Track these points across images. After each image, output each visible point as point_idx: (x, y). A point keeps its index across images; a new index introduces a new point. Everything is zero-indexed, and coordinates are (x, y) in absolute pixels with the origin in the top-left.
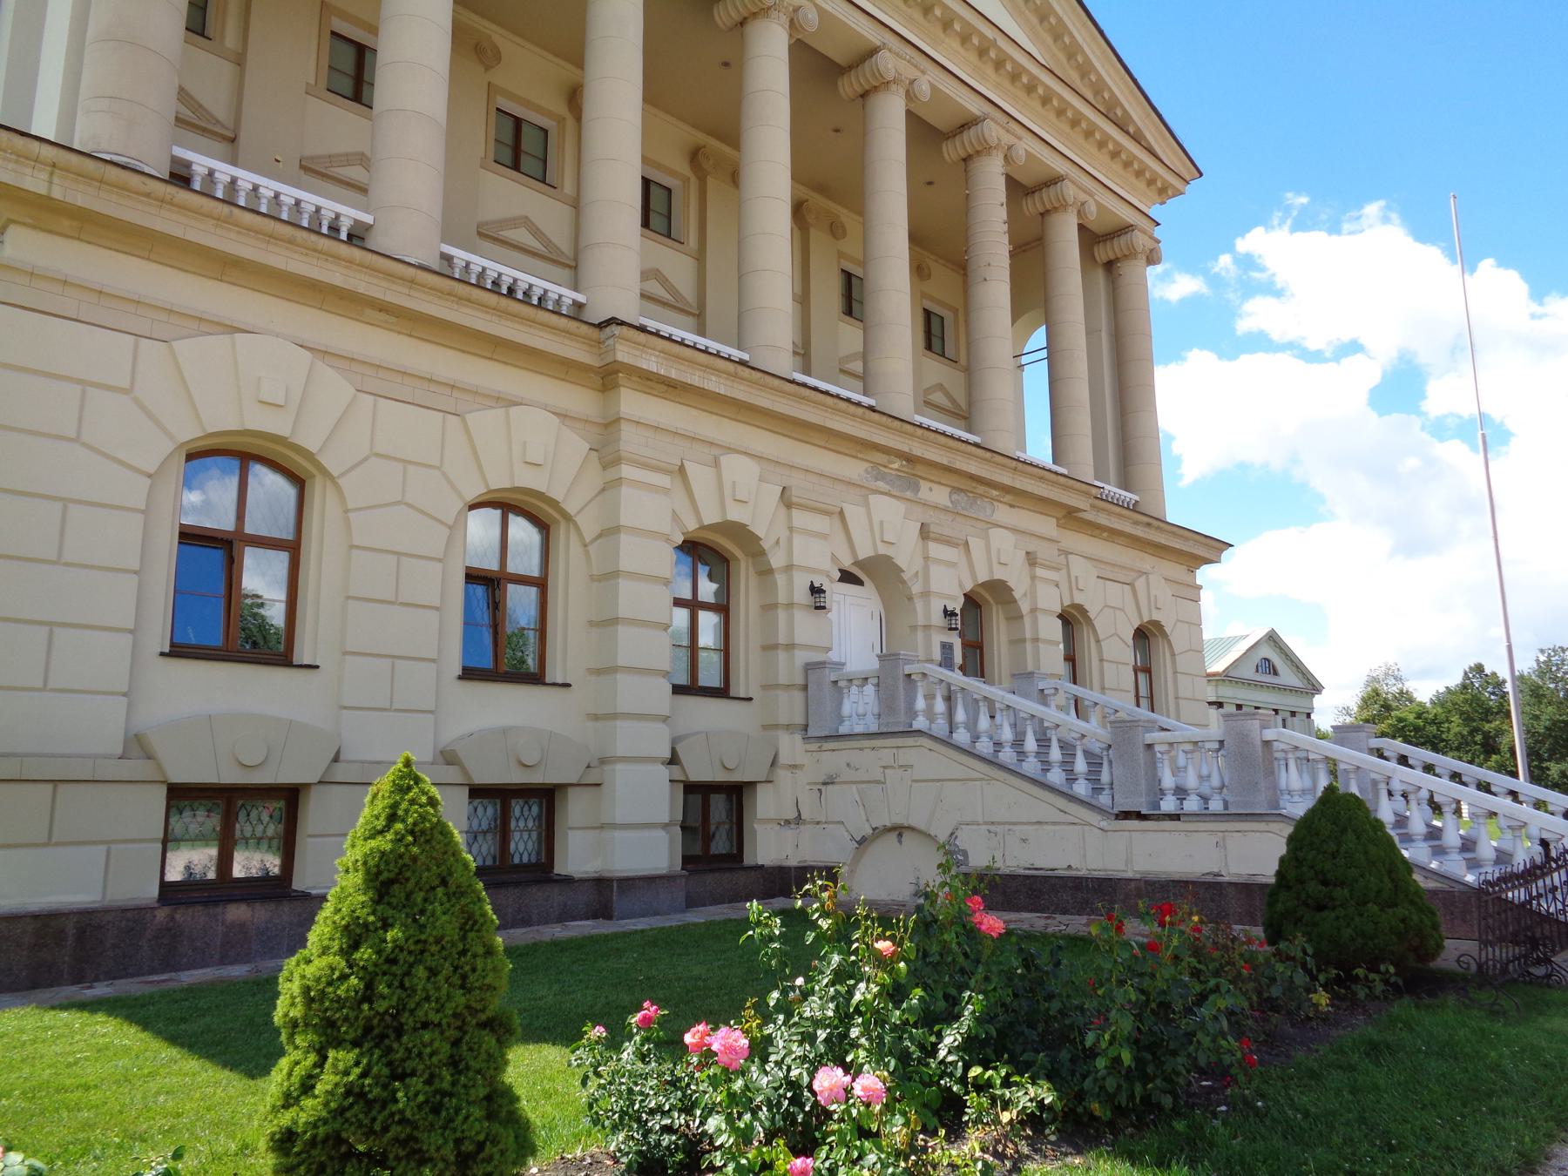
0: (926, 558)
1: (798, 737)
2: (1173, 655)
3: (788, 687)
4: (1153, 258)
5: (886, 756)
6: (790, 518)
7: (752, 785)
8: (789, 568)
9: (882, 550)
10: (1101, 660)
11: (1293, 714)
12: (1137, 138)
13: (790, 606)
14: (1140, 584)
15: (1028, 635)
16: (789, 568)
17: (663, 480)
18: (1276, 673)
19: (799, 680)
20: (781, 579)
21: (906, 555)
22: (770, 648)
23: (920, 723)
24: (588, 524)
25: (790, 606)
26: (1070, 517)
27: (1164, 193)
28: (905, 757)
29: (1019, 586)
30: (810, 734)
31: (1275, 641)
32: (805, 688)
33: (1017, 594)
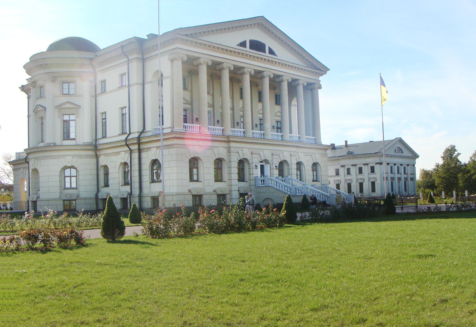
0: (273, 158)
1: (254, 186)
3: (253, 180)
4: (320, 87)
8: (252, 163)
11: (408, 165)
13: (253, 168)
14: (313, 156)
15: (290, 168)
16: (252, 163)
19: (254, 179)
20: (251, 164)
21: (269, 159)
22: (250, 174)
23: (270, 185)
24: (227, 161)
25: (253, 168)
27: (322, 75)
30: (256, 186)
32: (255, 180)
33: (288, 162)
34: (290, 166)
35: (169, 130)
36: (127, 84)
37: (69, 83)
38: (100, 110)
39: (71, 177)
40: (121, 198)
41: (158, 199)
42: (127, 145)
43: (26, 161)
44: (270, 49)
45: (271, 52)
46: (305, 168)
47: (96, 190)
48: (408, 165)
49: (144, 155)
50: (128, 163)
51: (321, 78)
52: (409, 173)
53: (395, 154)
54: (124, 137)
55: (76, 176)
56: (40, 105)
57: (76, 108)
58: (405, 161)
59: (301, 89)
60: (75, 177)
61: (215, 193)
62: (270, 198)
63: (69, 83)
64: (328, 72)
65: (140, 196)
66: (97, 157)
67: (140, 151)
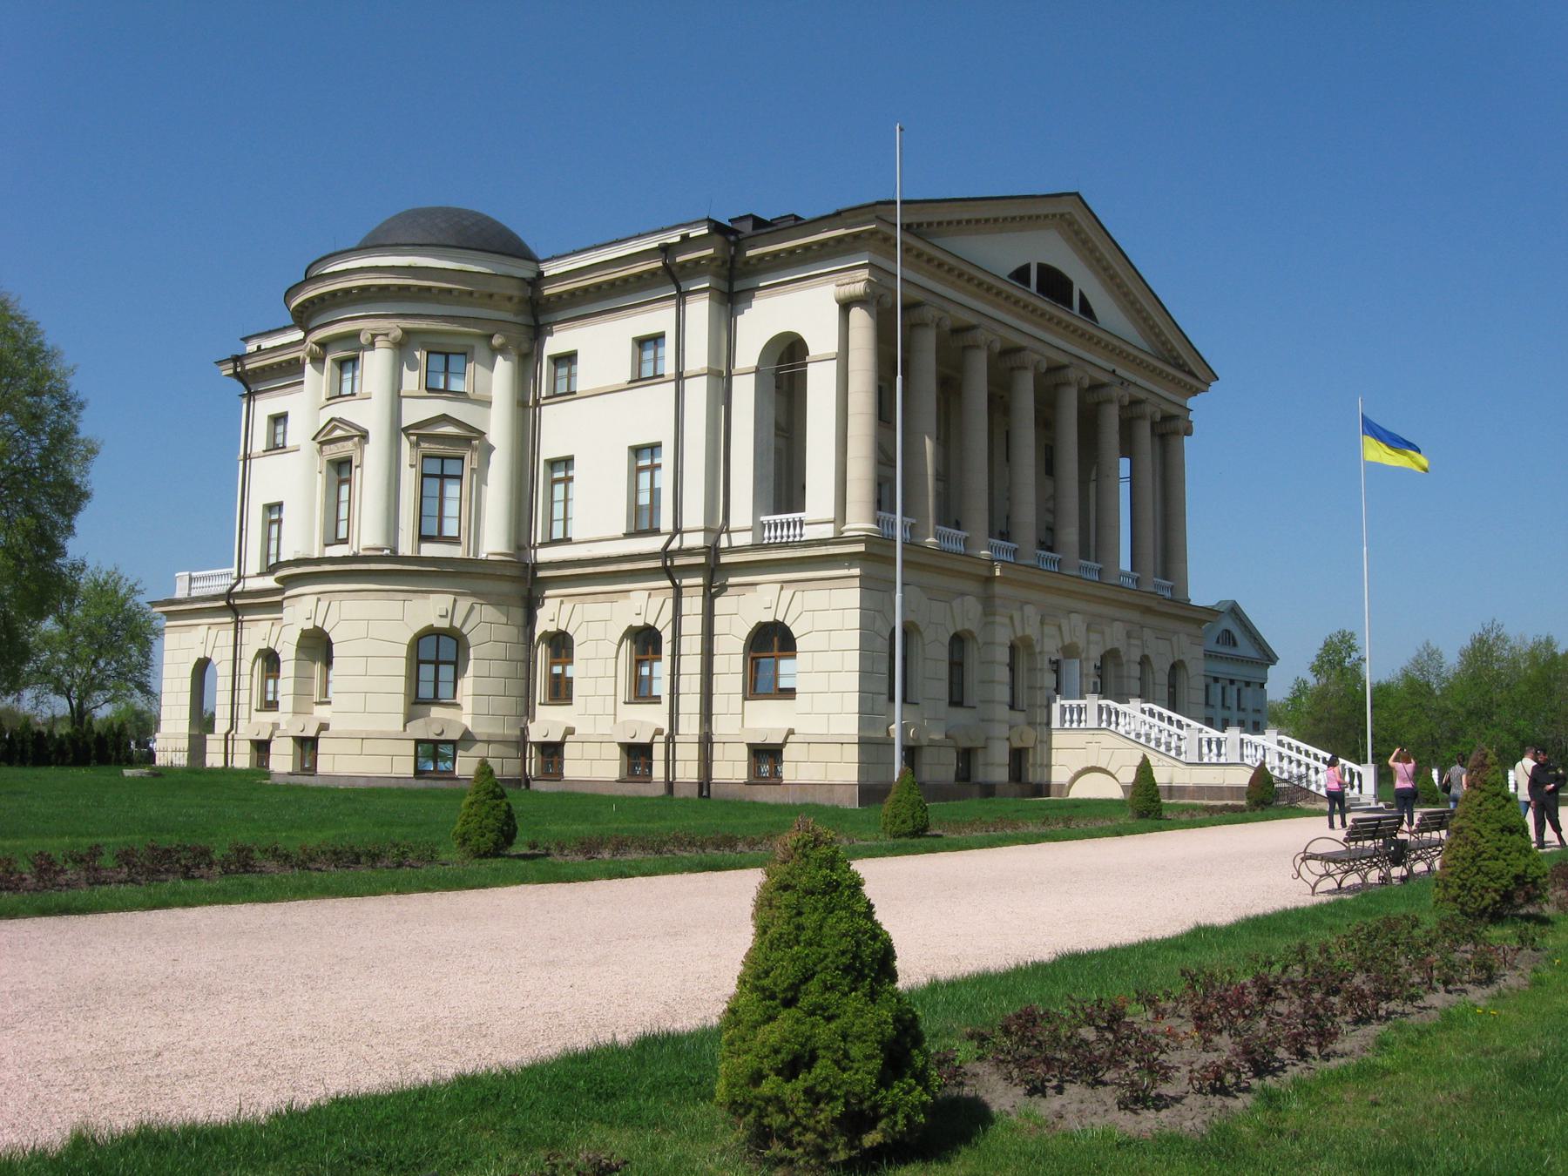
0: (1088, 643)
2: (1188, 678)
3: (1040, 706)
4: (1188, 432)
5: (1090, 738)
6: (1042, 628)
7: (1027, 749)
9: (1075, 639)
10: (1154, 684)
11: (1248, 684)
12: (1181, 367)
14: (1174, 639)
15: (1125, 674)
16: (1040, 653)
17: (1007, 621)
18: (1235, 644)
20: (1039, 658)
21: (1081, 644)
26: (1147, 610)
28: (1097, 738)
29: (1123, 650)
31: (1236, 614)
34: (1125, 667)
35: (828, 531)
36: (669, 368)
37: (447, 355)
38: (549, 448)
39: (437, 663)
40: (621, 745)
41: (781, 752)
42: (669, 572)
43: (228, 602)
44: (1082, 295)
45: (1086, 309)
46: (1154, 679)
47: (521, 709)
48: (1248, 684)
49: (720, 604)
50: (659, 627)
51: (1191, 403)
52: (1250, 707)
53: (1220, 649)
54: (654, 544)
55: (455, 664)
56: (341, 420)
58: (1241, 672)
59: (1144, 431)
60: (452, 667)
61: (952, 743)
62: (1104, 766)
63: (447, 355)
64: (1212, 384)
65: (706, 742)
66: (531, 605)
67: (711, 593)
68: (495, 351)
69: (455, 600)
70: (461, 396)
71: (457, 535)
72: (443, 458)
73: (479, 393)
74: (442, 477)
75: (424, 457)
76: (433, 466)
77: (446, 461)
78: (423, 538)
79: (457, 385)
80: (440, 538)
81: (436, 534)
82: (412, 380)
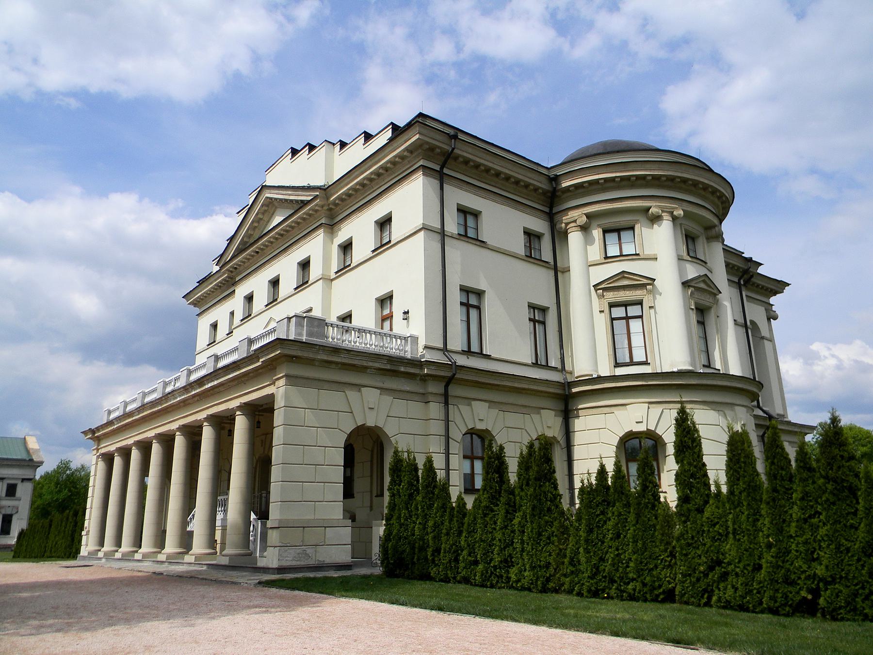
57: (644, 286)
63: (618, 231)
68: (655, 219)
69: (649, 408)
70: (635, 257)
71: (645, 360)
72: (625, 305)
73: (648, 252)
74: (627, 318)
75: (612, 305)
76: (619, 312)
77: (628, 308)
78: (617, 365)
79: (628, 249)
80: (632, 363)
81: (629, 361)
82: (595, 252)
